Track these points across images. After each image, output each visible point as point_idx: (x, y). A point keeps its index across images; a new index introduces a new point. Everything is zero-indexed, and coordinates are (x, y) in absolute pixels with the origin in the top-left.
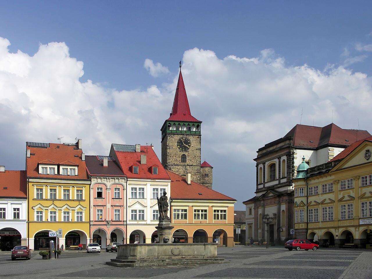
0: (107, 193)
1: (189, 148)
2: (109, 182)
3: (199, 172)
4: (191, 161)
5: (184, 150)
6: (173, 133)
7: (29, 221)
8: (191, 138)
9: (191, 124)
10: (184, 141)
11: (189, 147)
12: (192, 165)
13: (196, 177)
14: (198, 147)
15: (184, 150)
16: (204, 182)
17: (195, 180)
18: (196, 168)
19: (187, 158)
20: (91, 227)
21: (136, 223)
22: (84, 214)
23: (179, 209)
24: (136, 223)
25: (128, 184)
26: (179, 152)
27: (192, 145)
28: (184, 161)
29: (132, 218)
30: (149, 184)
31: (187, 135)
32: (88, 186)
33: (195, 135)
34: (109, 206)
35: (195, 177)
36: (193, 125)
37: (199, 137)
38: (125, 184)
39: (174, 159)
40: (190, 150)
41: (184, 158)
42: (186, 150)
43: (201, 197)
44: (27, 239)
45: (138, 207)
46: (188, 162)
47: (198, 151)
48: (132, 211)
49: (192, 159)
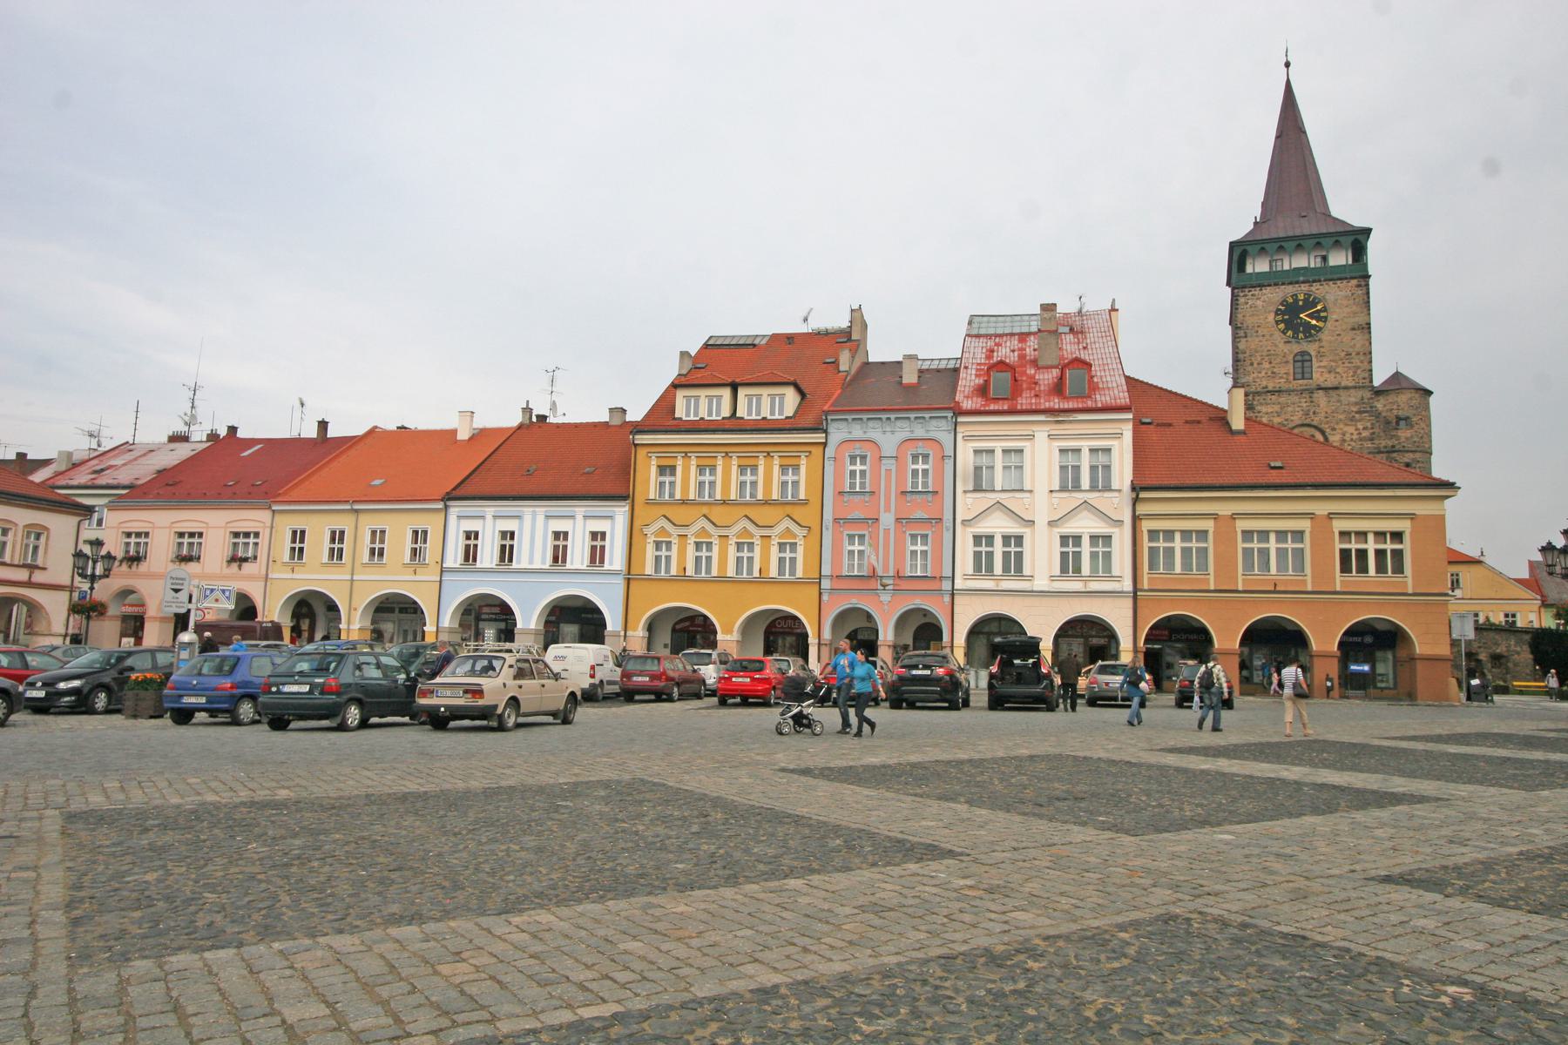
0: (883, 472)
1: (1321, 328)
2: (893, 432)
3: (1366, 410)
4: (1330, 372)
5: (1301, 335)
6: (1262, 282)
7: (629, 574)
8: (1334, 295)
9: (1327, 242)
10: (1301, 303)
11: (1320, 324)
12: (1336, 388)
13: (1357, 429)
14: (1361, 320)
15: (1301, 335)
16: (1393, 446)
17: (1352, 440)
18: (1354, 396)
19: (1315, 364)
20: (825, 597)
21: (988, 584)
22: (800, 549)
23: (1173, 532)
24: (988, 584)
25: (959, 436)
26: (1281, 345)
27: (1335, 317)
28: (1303, 373)
29: (977, 568)
30: (1041, 434)
31: (1314, 281)
32: (817, 451)
33: (1346, 278)
34: (887, 520)
35: (1351, 429)
36: (1337, 244)
38: (946, 439)
40: (1326, 332)
42: (1311, 335)
43: (1274, 477)
44: (622, 633)
45: (998, 525)
46: (1319, 376)
47: (1359, 338)
48: (977, 539)
49: (1338, 367)
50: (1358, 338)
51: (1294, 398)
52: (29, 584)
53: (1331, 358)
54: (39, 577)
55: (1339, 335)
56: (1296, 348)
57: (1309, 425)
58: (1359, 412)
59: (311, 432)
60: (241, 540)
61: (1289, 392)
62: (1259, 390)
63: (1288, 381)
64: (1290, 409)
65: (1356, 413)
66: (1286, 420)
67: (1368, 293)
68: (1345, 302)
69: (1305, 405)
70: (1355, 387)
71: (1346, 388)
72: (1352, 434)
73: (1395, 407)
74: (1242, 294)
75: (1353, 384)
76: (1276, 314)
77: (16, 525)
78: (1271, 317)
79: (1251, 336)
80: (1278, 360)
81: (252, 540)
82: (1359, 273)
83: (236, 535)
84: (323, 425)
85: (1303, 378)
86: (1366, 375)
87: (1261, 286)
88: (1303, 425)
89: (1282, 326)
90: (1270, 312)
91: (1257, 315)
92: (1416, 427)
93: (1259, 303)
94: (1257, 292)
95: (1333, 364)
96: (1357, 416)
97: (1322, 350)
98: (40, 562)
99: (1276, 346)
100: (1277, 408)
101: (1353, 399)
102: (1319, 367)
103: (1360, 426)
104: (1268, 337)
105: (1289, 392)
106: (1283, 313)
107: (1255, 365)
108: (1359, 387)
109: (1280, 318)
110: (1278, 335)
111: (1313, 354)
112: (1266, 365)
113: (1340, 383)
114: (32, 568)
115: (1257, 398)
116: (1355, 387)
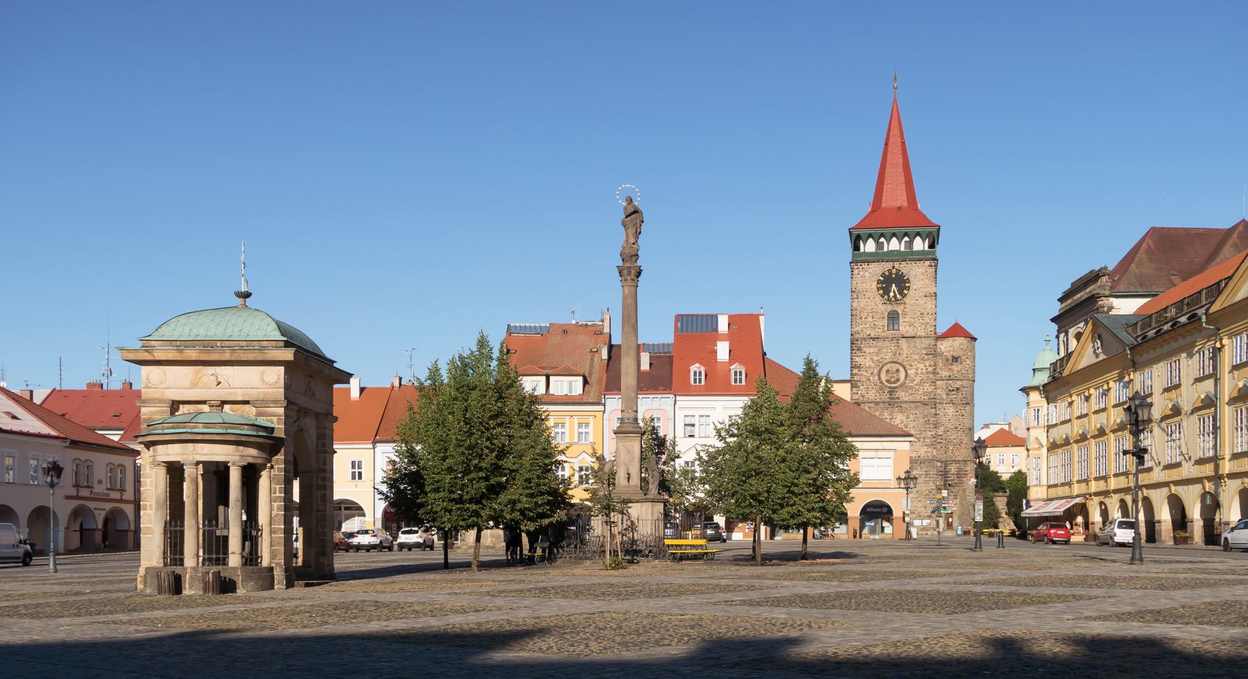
1: (906, 295)
3: (933, 353)
10: (894, 276)
12: (914, 337)
13: (925, 366)
14: (932, 290)
16: (950, 376)
18: (927, 342)
19: (901, 320)
26: (880, 306)
35: (921, 366)
37: (933, 264)
39: (868, 324)
41: (893, 318)
46: (904, 328)
47: (930, 304)
49: (915, 322)
50: (928, 303)
51: (887, 343)
53: (911, 316)
55: (917, 300)
56: (890, 308)
57: (896, 363)
58: (926, 354)
61: (885, 339)
62: (865, 336)
63: (884, 331)
64: (884, 351)
65: (926, 354)
66: (882, 358)
67: (936, 271)
68: (922, 277)
69: (893, 348)
70: (925, 337)
71: (920, 337)
72: (922, 369)
73: (952, 349)
74: (855, 267)
75: (923, 334)
76: (878, 283)
78: (876, 283)
79: (861, 298)
80: (878, 316)
82: (930, 257)
85: (893, 330)
86: (932, 329)
87: (868, 262)
88: (892, 362)
89: (881, 292)
90: (874, 281)
91: (866, 283)
92: (964, 363)
93: (867, 274)
94: (865, 265)
95: (912, 320)
96: (926, 357)
97: (905, 310)
99: (877, 305)
100: (876, 350)
101: (923, 346)
102: (904, 322)
103: (928, 365)
104: (871, 299)
105: (885, 339)
106: (882, 282)
107: (863, 319)
108: (928, 337)
109: (880, 286)
110: (878, 298)
111: (900, 312)
112: (870, 319)
113: (916, 334)
115: (863, 342)
116: (925, 337)
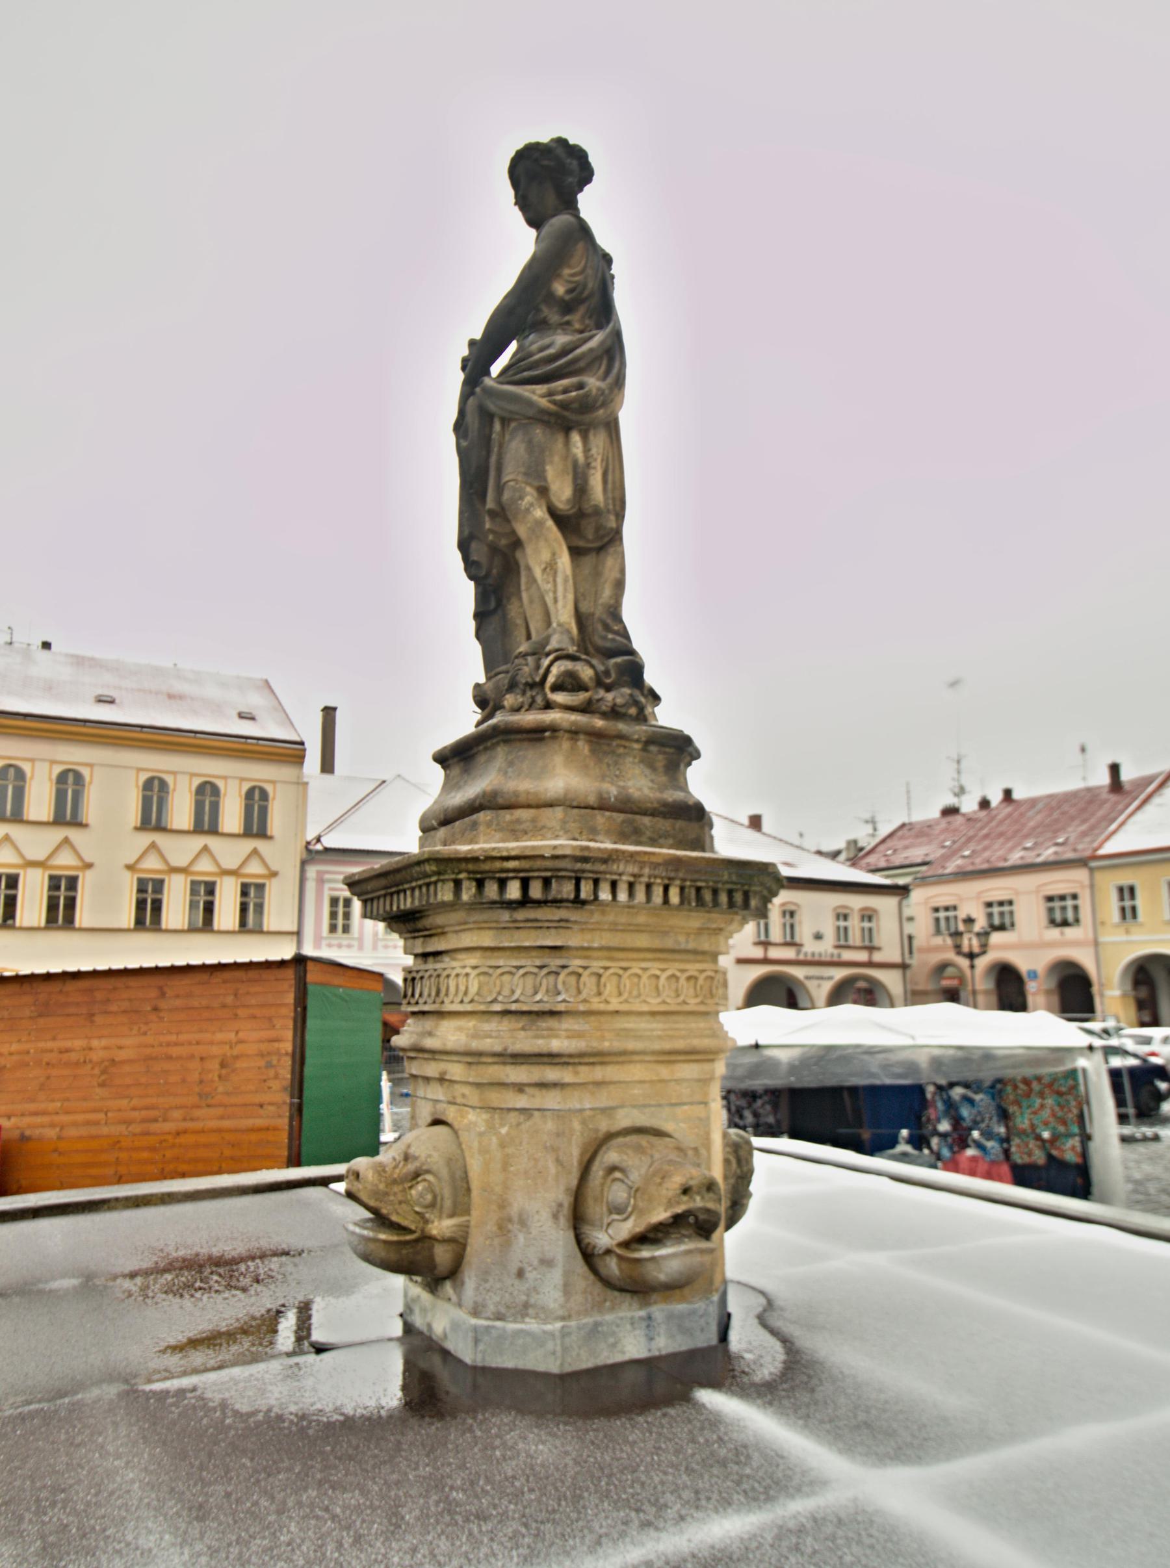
52: (870, 964)
54: (878, 957)
59: (1105, 779)
60: (1057, 904)
77: (852, 909)
81: (1069, 903)
83: (1050, 899)
84: (1115, 769)
98: (876, 943)
114: (871, 949)
